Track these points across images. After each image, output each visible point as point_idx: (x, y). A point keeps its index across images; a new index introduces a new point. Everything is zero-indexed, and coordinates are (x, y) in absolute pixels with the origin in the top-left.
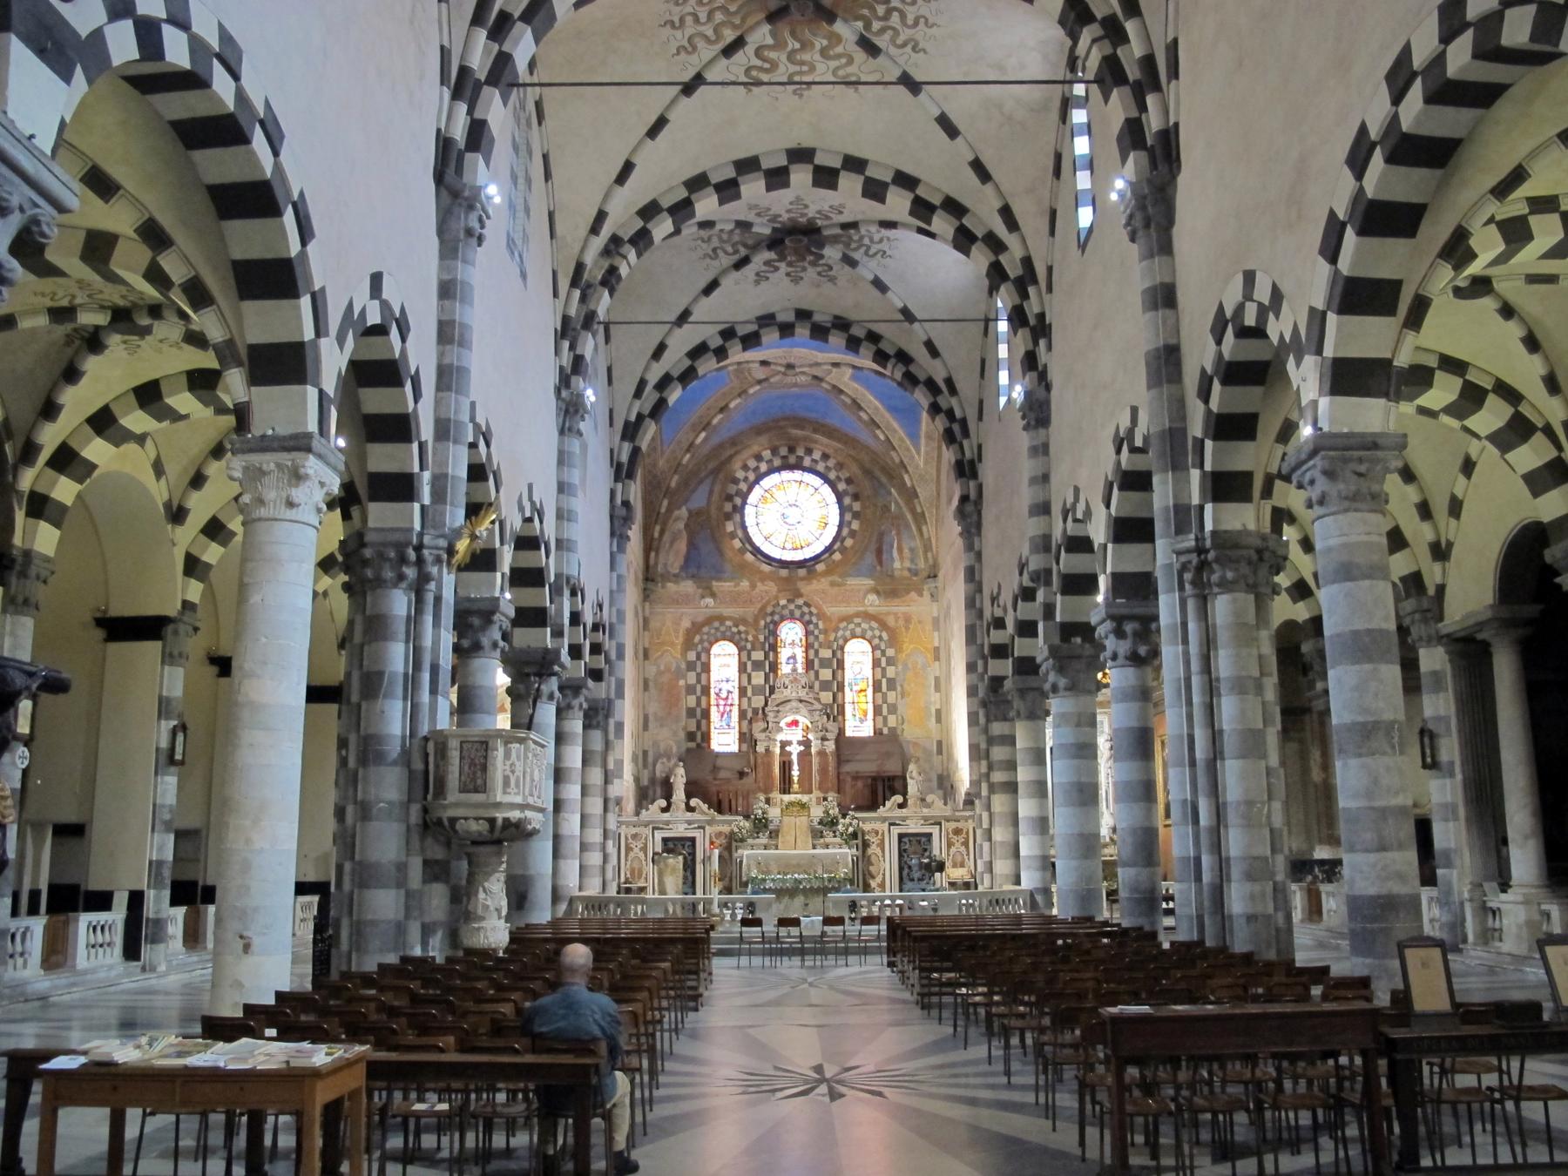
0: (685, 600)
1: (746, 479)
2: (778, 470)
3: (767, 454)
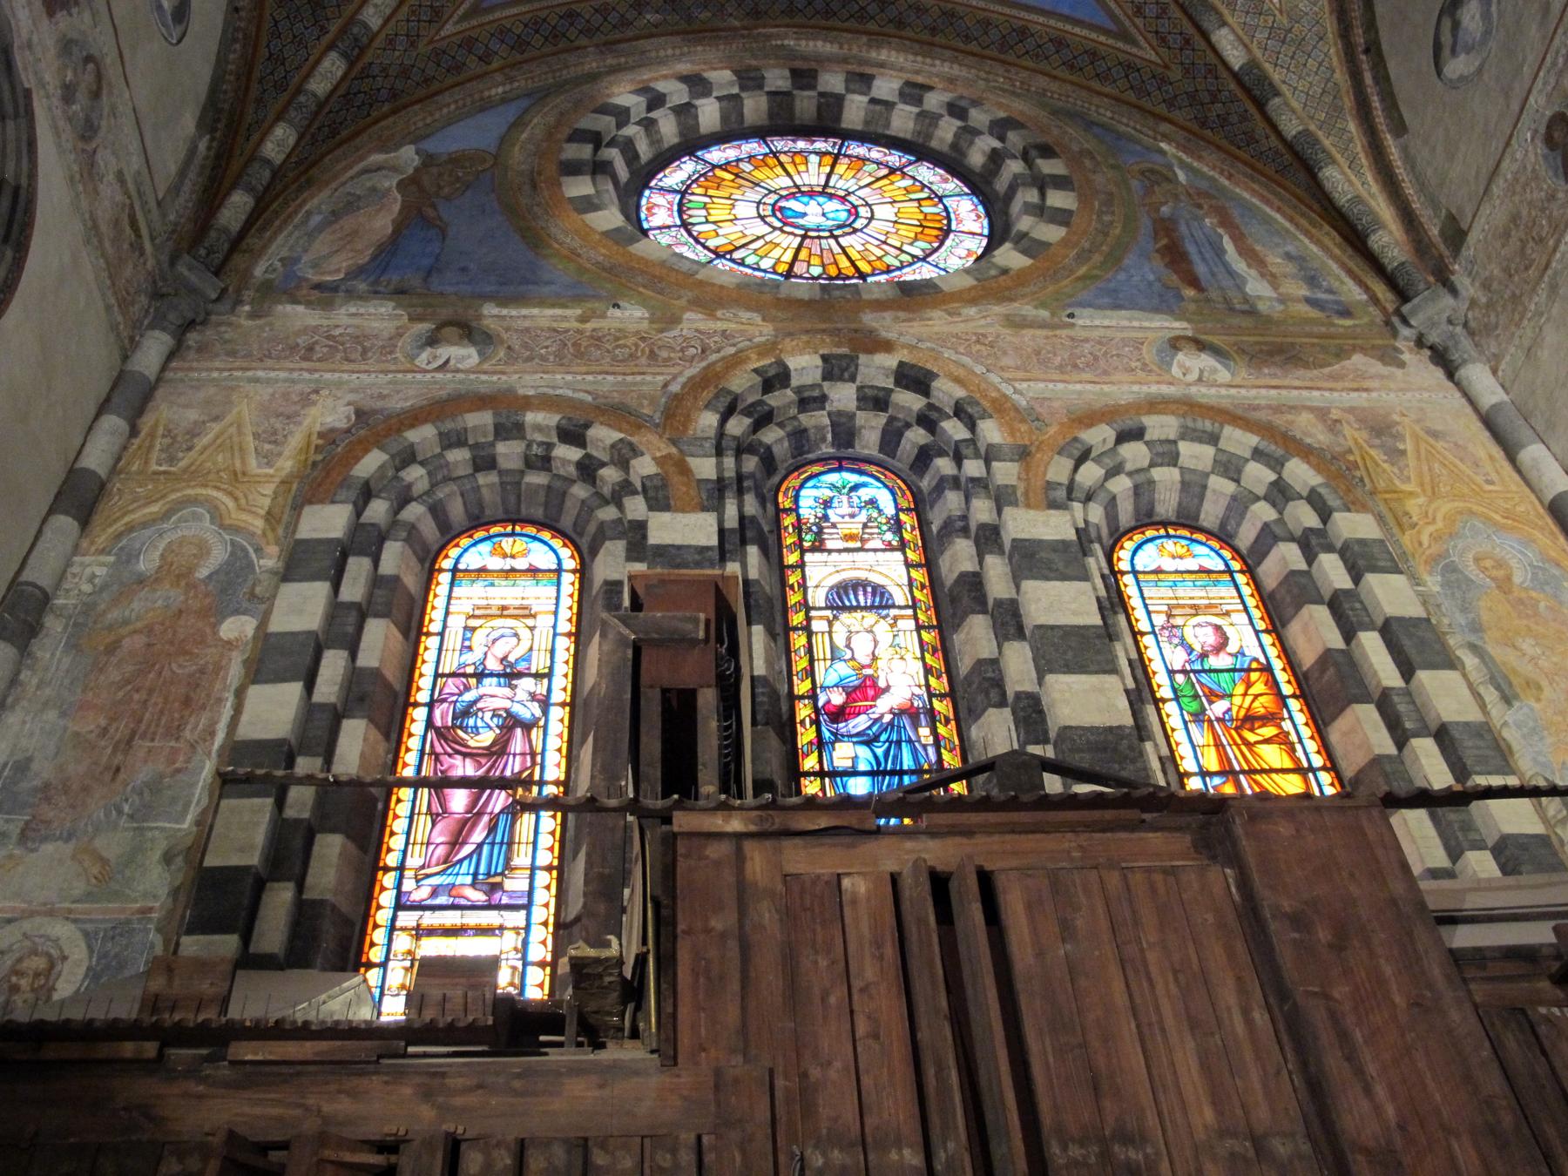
0: (358, 348)
1: (649, 125)
2: (761, 133)
3: (722, 78)
